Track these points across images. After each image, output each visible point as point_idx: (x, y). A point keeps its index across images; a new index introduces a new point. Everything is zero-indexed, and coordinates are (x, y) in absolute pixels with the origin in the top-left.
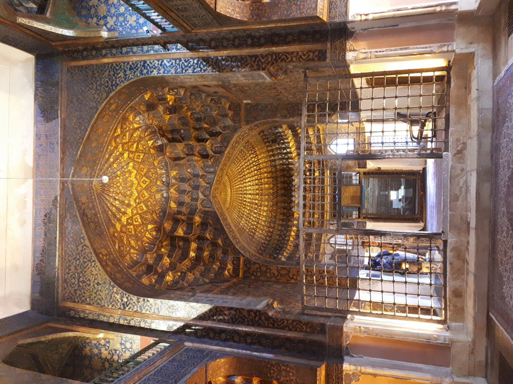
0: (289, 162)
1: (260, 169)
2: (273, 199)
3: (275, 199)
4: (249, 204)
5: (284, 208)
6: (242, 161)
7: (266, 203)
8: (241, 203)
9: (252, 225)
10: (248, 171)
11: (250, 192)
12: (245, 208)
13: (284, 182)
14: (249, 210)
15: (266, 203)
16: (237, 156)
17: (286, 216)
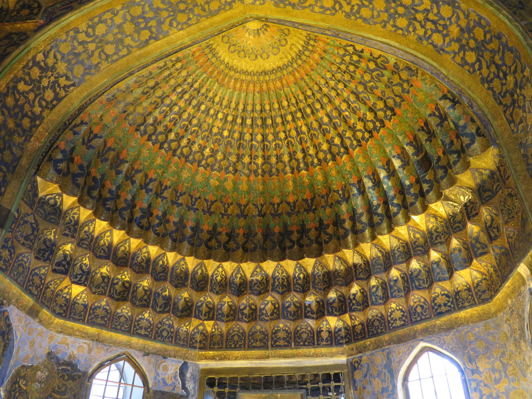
0: (363, 231)
1: (334, 159)
2: (256, 206)
3: (256, 213)
4: (236, 135)
5: (231, 236)
6: (352, 85)
7: (243, 186)
8: (236, 109)
9: (179, 138)
10: (326, 120)
11: (271, 137)
12: (225, 119)
13: (303, 231)
14: (221, 134)
15: (243, 186)
16: (366, 54)
17: (209, 240)
